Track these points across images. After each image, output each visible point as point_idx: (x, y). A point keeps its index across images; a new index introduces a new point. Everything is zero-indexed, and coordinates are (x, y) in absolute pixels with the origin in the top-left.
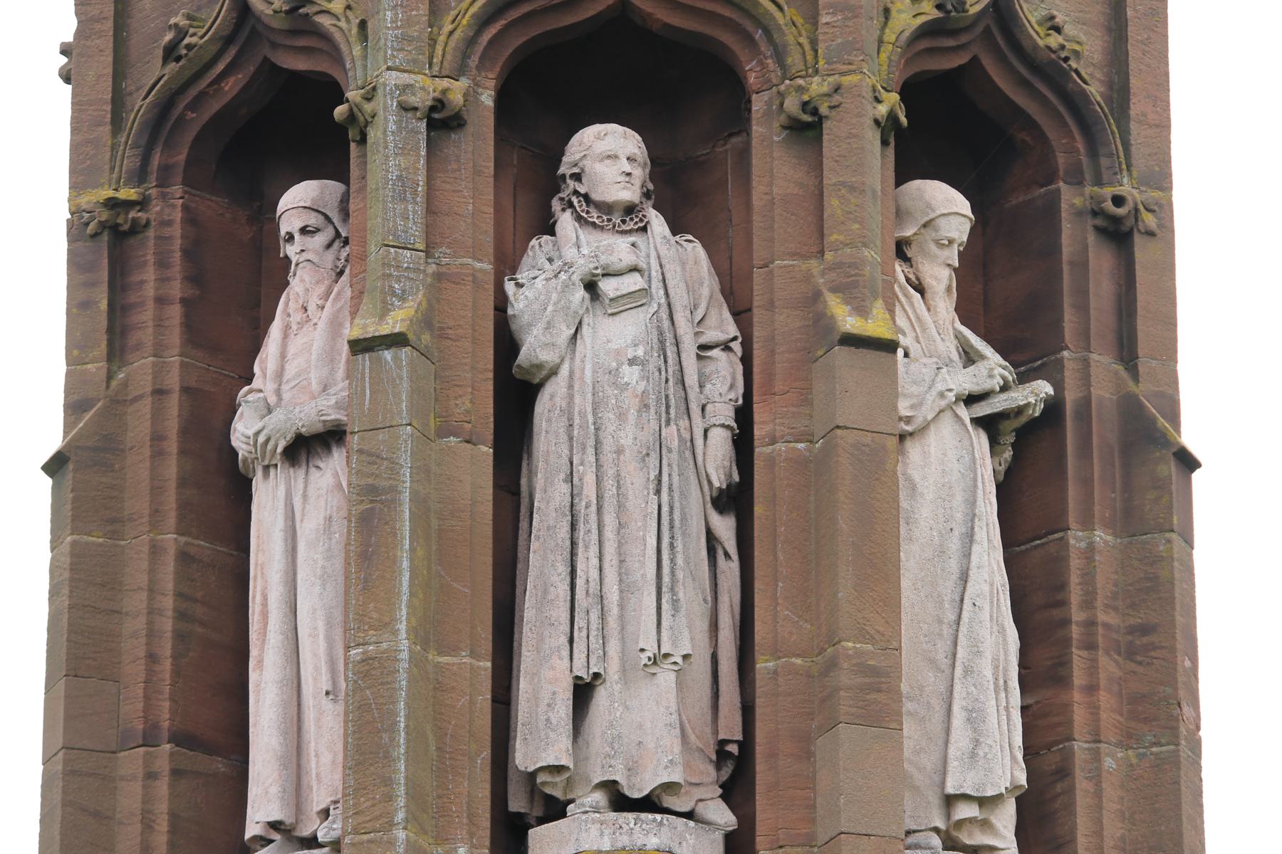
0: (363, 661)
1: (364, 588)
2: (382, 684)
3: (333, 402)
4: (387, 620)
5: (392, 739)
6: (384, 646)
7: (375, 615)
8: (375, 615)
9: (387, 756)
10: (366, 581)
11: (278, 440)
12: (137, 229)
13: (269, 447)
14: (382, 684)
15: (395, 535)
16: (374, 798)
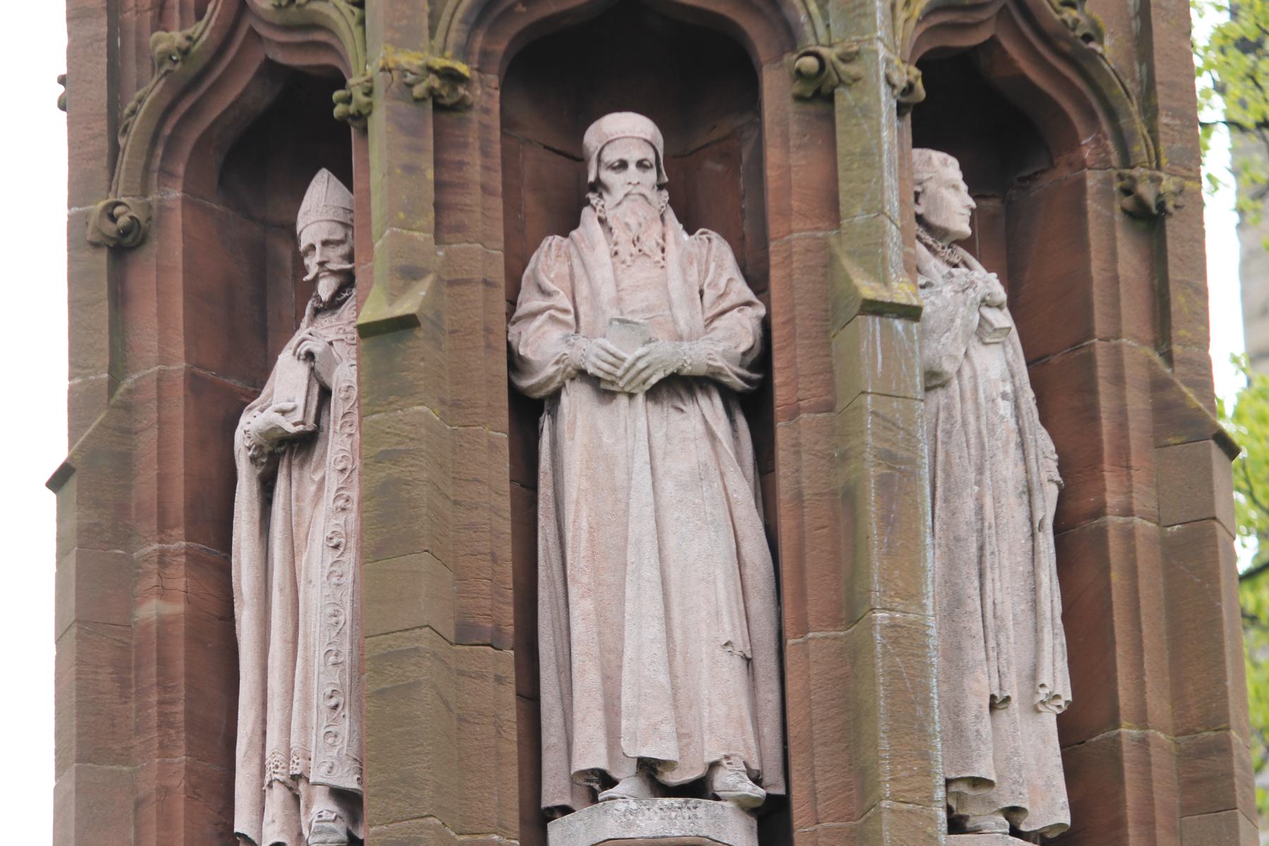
0: (892, 626)
1: (888, 553)
2: (913, 655)
3: (720, 349)
4: (914, 592)
5: (928, 715)
6: (911, 617)
7: (901, 584)
8: (901, 584)
9: (922, 730)
10: (889, 547)
11: (657, 370)
12: (461, 106)
13: (644, 375)
14: (913, 655)
15: (916, 508)
16: (911, 769)
